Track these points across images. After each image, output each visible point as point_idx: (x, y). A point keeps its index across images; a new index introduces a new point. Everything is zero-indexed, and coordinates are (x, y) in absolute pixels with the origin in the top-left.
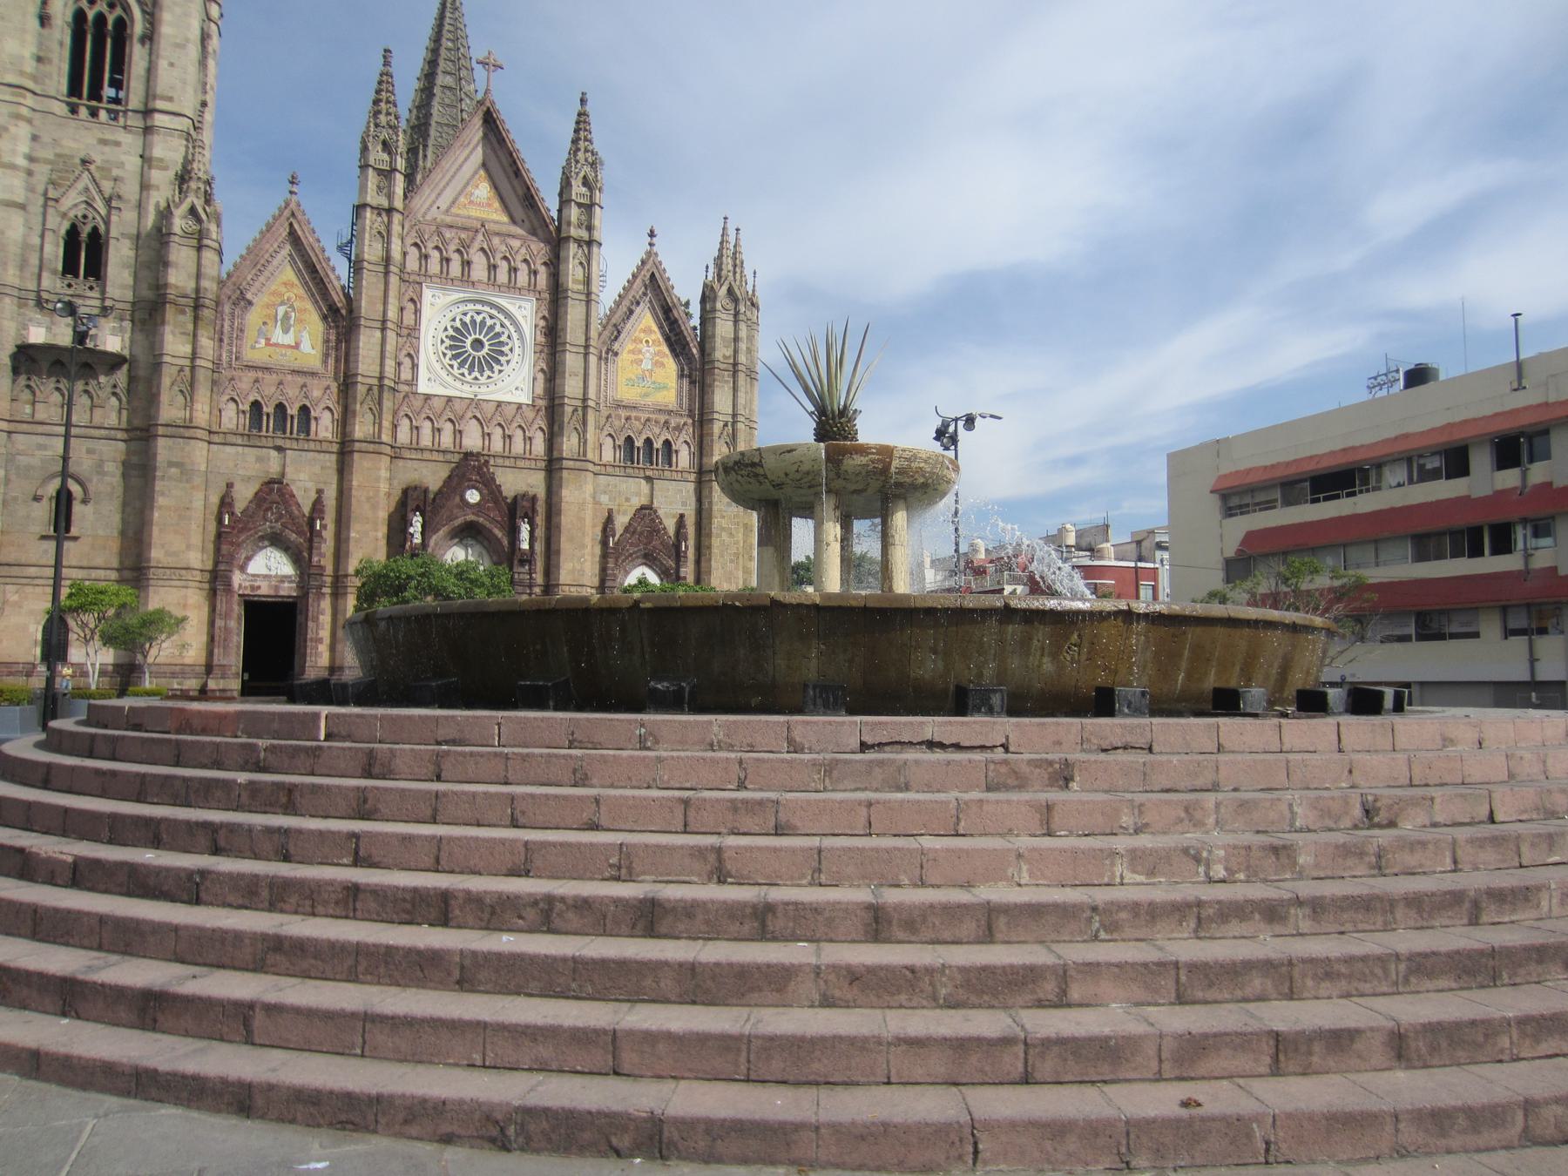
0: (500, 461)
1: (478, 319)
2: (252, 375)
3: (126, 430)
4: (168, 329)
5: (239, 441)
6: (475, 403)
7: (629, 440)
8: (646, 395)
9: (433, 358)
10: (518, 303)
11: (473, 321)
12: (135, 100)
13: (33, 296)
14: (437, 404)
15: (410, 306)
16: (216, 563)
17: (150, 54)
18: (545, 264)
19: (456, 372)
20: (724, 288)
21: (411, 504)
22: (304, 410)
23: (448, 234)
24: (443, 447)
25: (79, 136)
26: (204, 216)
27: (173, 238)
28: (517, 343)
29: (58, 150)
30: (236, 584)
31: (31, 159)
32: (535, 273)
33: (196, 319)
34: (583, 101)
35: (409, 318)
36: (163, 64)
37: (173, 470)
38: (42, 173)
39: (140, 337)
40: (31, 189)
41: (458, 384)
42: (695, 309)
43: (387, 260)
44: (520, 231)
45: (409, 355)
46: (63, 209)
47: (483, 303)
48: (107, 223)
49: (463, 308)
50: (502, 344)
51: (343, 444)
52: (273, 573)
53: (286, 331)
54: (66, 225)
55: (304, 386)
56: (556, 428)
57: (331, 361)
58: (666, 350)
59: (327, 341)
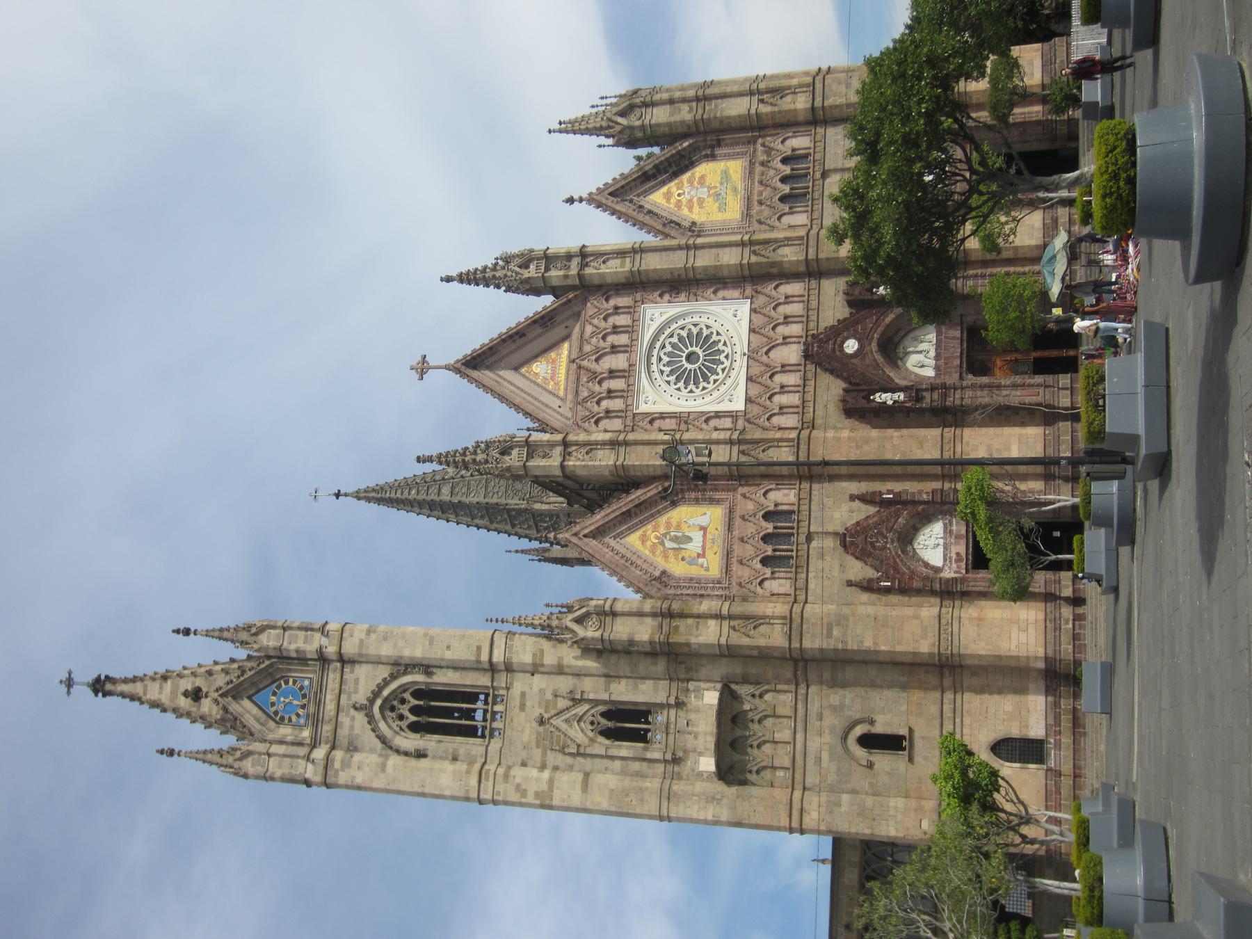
0: (812, 325)
1: (666, 359)
2: (735, 567)
3: (797, 685)
4: (693, 640)
5: (804, 576)
6: (751, 356)
7: (783, 199)
8: (735, 190)
9: (708, 398)
10: (647, 321)
11: (669, 364)
12: (483, 680)
13: (670, 768)
14: (755, 390)
15: (657, 424)
16: (933, 593)
17: (441, 667)
18: (607, 300)
20: (620, 120)
21: (863, 403)
22: (767, 516)
23: (586, 394)
24: (800, 382)
25: (520, 726)
26: (584, 610)
27: (606, 636)
28: (688, 320)
29: (533, 745)
30: (953, 575)
31: (543, 767)
32: (616, 308)
33: (682, 615)
34: (448, 279)
35: (670, 424)
36: (448, 655)
37: (835, 633)
38: (554, 758)
39: (703, 673)
40: (571, 768)
41: (733, 374)
42: (643, 152)
43: (613, 444)
44: (577, 330)
45: (707, 421)
46: (586, 741)
47: (649, 356)
48: (596, 703)
49: (656, 375)
50: (690, 335)
51: (801, 478)
52: (941, 541)
53: (689, 539)
54: (601, 739)
55: (743, 518)
56: (774, 271)
57: (717, 495)
58: (688, 174)
59: (697, 501)
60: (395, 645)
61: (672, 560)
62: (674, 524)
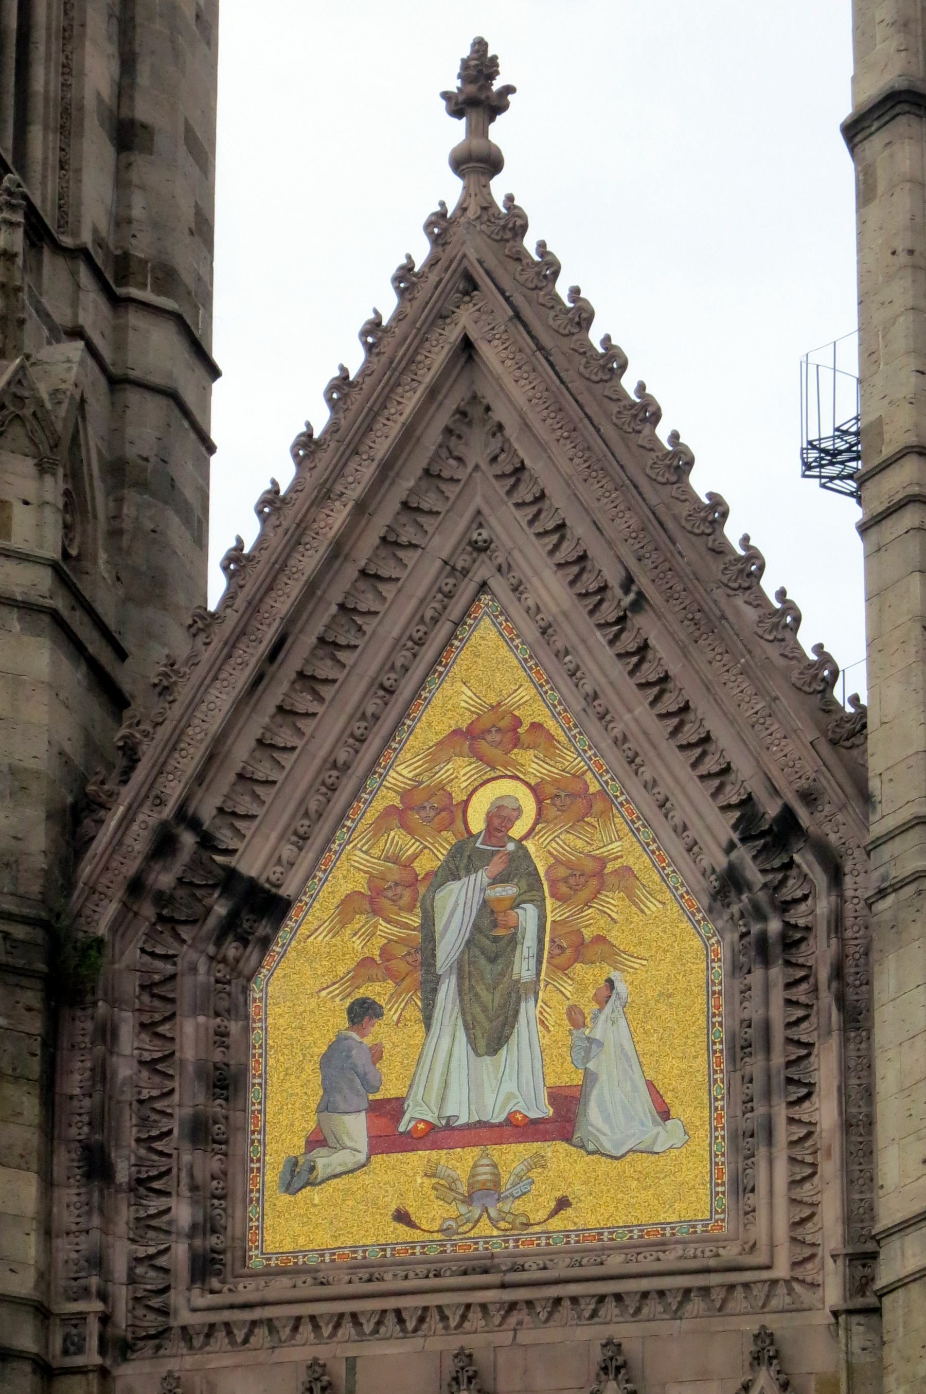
53: (492, 1033)
61: (356, 944)
62: (592, 923)
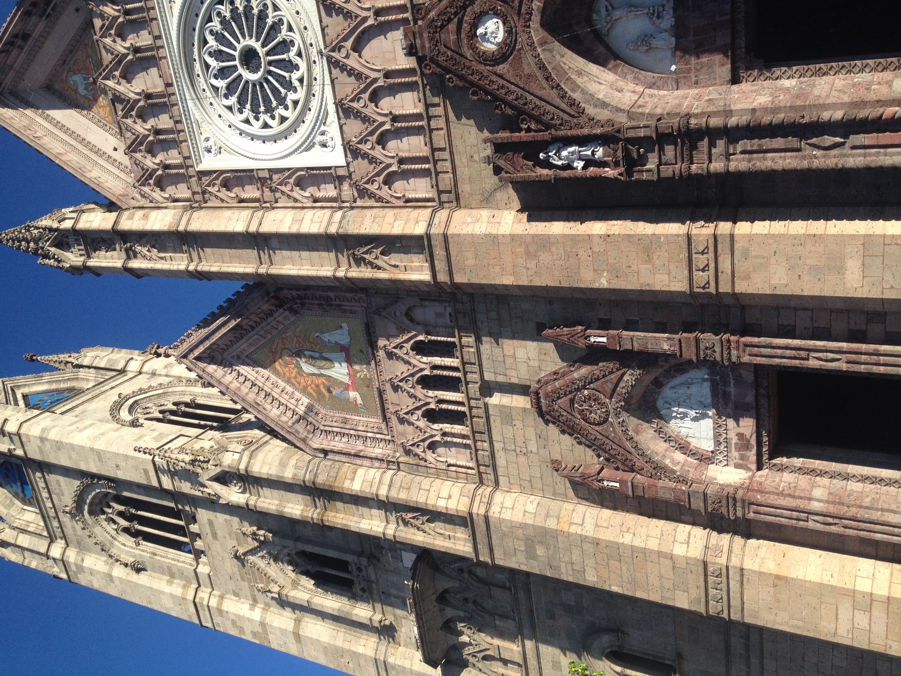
14: (355, 127)
19: (300, 95)
27: (251, 503)
29: (239, 578)
37: (539, 552)
41: (317, 89)
60: (70, 458)
